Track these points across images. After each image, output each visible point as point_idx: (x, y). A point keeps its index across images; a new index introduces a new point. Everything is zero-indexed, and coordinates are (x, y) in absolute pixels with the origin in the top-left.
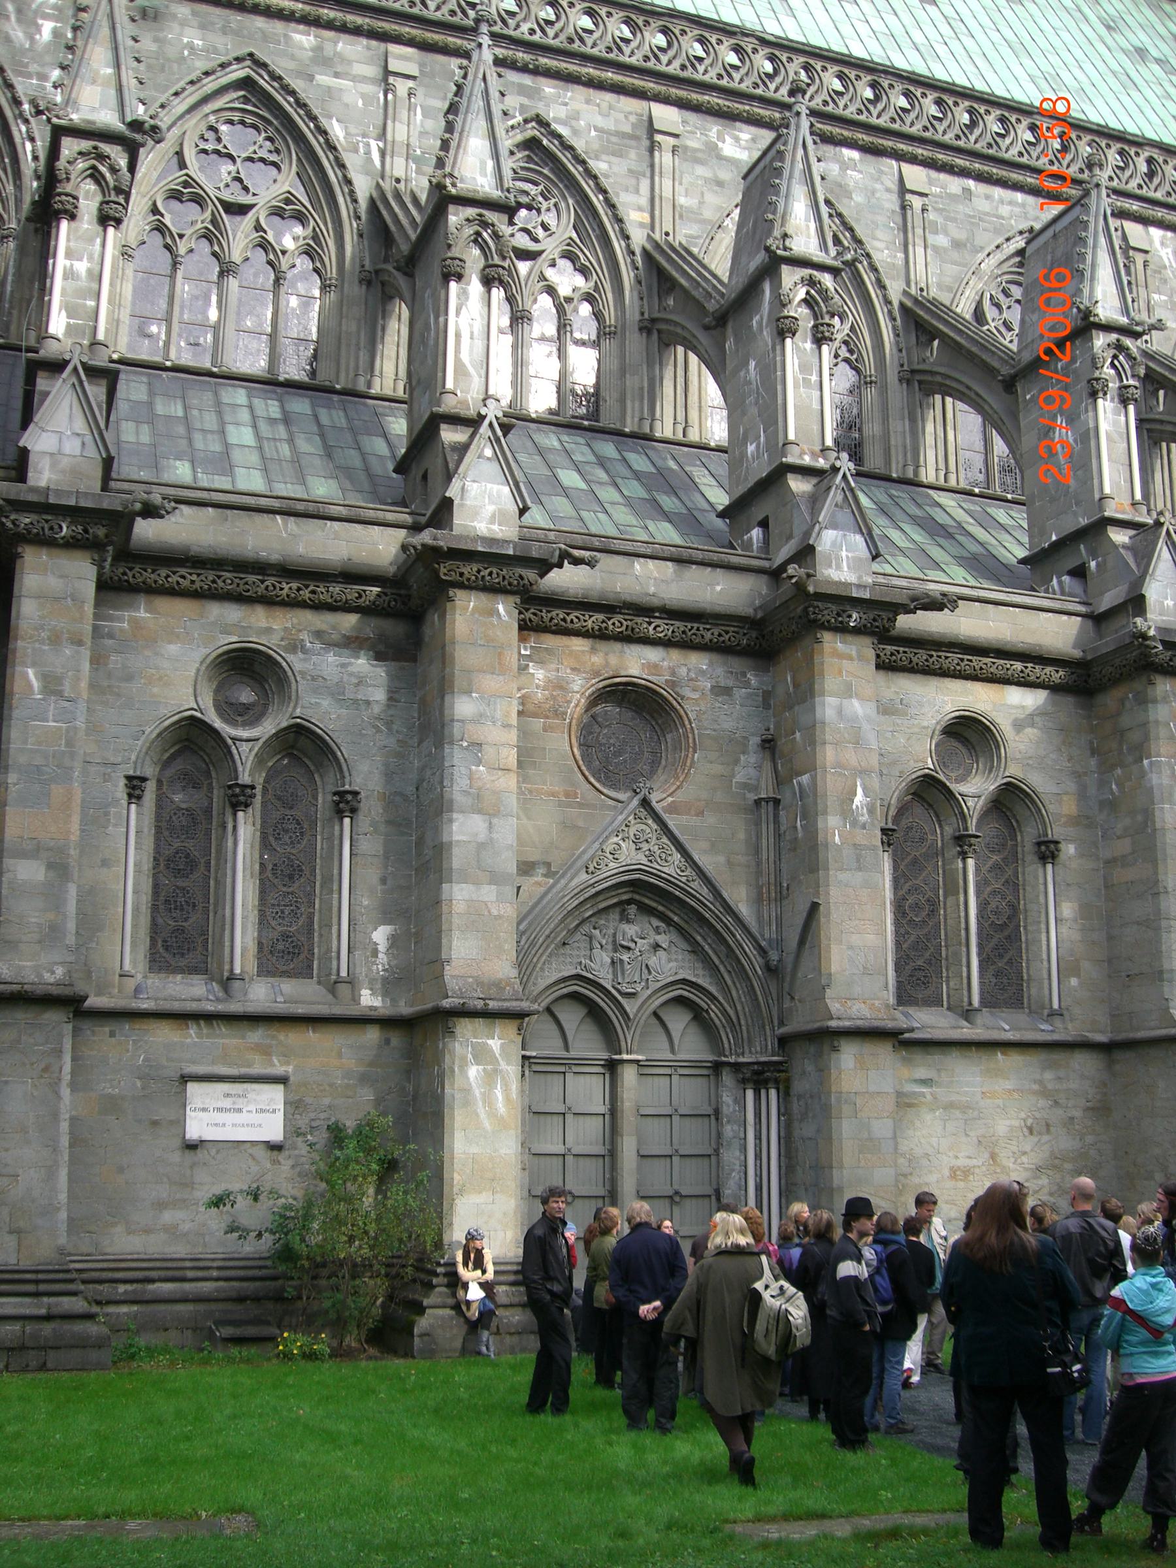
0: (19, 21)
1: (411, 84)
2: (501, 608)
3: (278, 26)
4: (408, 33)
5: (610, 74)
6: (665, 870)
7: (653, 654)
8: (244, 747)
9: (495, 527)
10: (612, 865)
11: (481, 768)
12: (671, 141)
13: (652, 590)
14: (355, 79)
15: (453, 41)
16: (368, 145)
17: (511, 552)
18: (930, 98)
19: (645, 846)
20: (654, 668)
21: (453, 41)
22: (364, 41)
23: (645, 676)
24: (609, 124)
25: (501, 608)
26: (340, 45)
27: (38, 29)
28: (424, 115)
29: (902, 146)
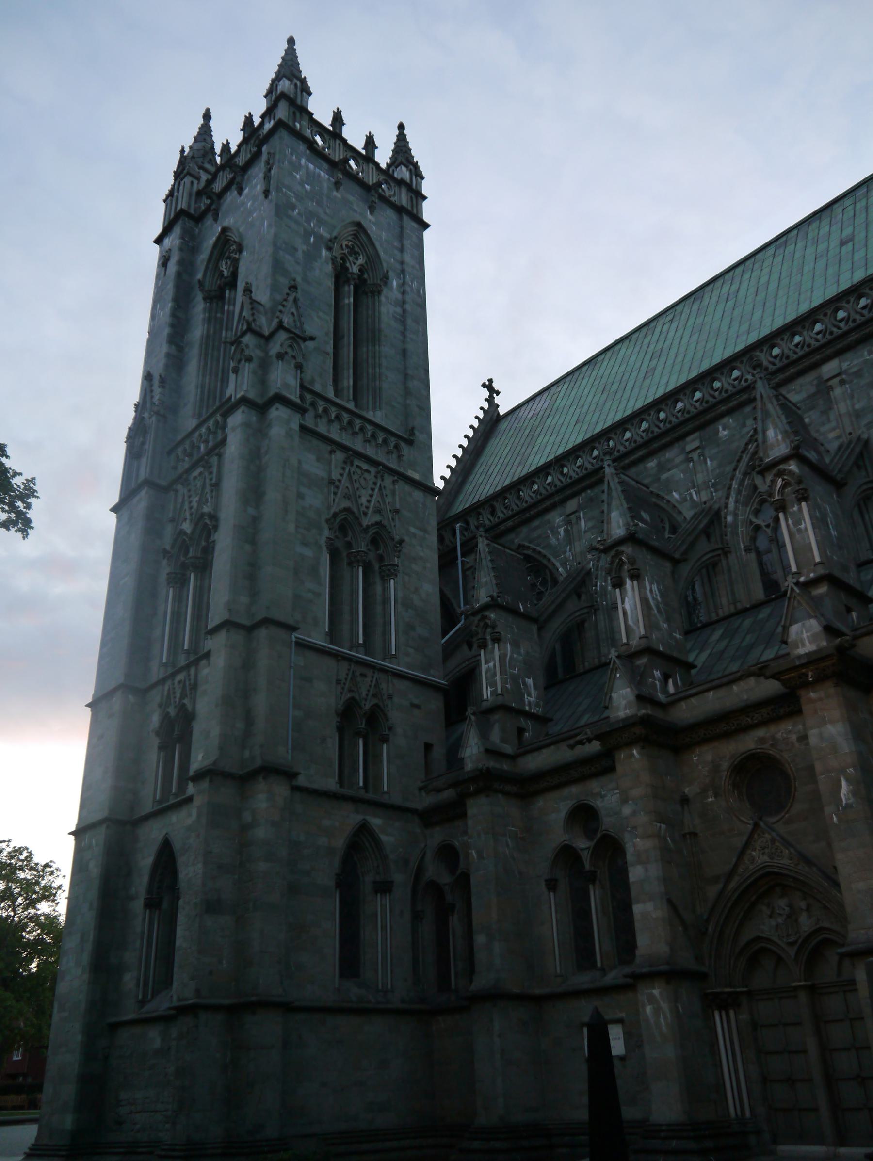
0: (553, 535)
1: (699, 451)
2: (635, 752)
3: (641, 467)
4: (779, 380)
5: (792, 370)
6: (781, 862)
7: (761, 733)
8: (586, 852)
9: (627, 711)
10: (751, 867)
11: (638, 839)
12: (837, 380)
13: (745, 697)
14: (676, 466)
15: (781, 377)
16: (691, 494)
17: (621, 725)
18: (682, 395)
19: (767, 851)
20: (762, 740)
21: (781, 377)
22: (676, 445)
23: (759, 747)
24: (803, 395)
25: (635, 752)
26: (667, 454)
27: (559, 533)
28: (711, 461)
29: (632, 458)
